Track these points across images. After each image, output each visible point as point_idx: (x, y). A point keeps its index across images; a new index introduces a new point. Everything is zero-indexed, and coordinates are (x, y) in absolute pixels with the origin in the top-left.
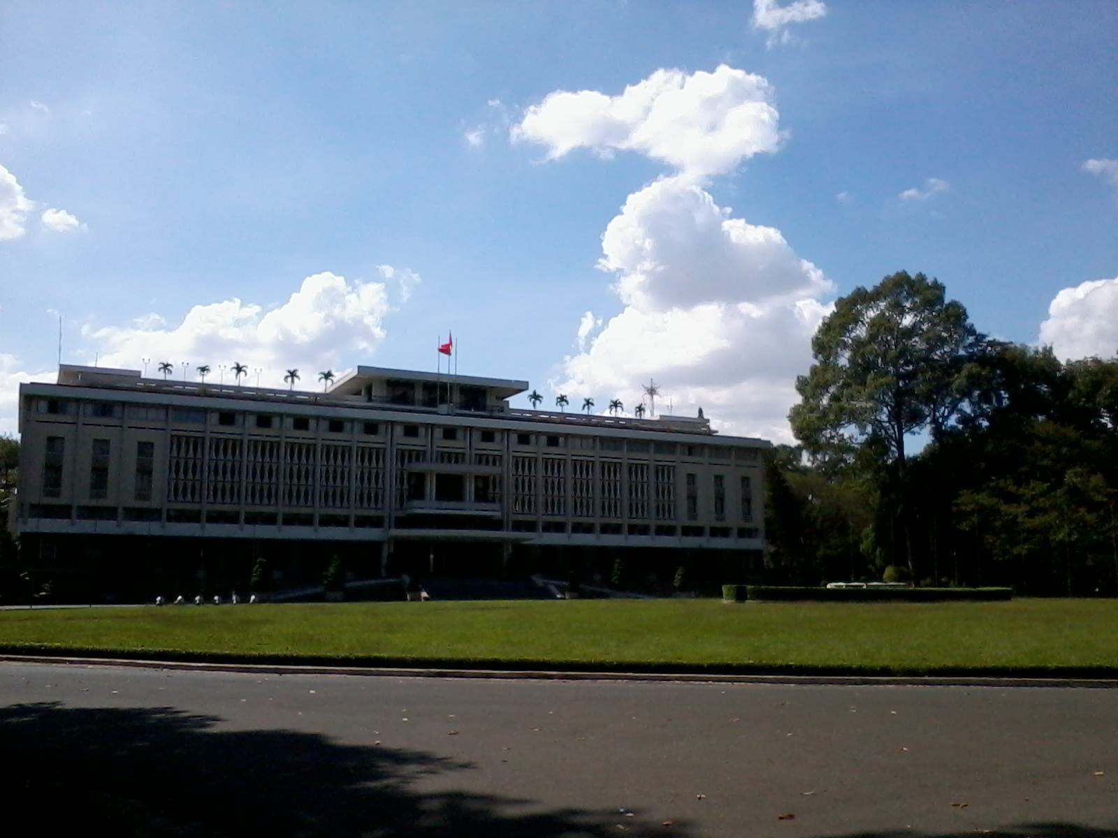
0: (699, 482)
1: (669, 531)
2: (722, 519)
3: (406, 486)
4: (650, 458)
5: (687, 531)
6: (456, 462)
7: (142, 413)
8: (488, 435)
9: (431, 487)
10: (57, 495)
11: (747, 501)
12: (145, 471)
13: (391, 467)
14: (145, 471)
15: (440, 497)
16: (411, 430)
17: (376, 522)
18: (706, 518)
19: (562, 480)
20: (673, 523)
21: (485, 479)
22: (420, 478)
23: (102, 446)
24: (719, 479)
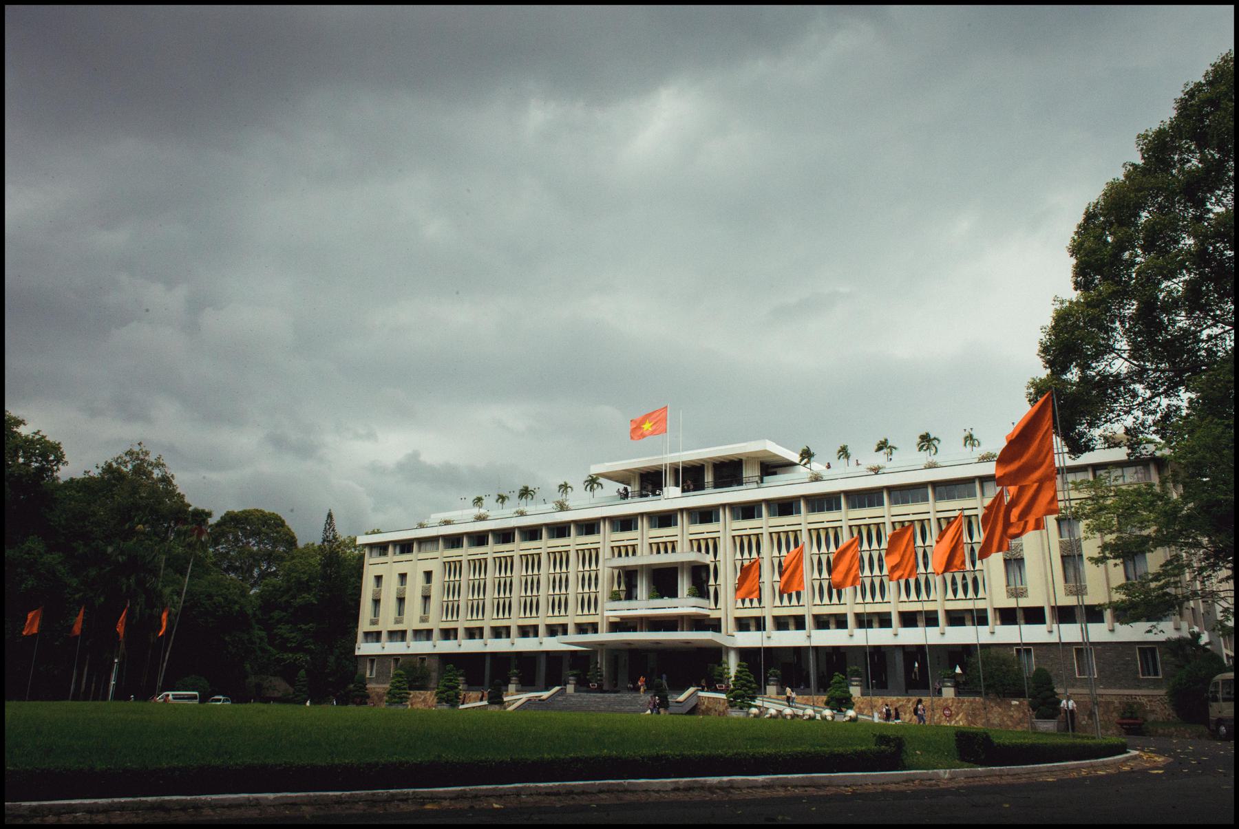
1: (980, 618)
2: (1080, 591)
3: (623, 587)
12: (426, 598)
13: (607, 567)
14: (426, 598)
15: (652, 596)
16: (626, 523)
20: (980, 605)
21: (707, 566)
23: (403, 576)
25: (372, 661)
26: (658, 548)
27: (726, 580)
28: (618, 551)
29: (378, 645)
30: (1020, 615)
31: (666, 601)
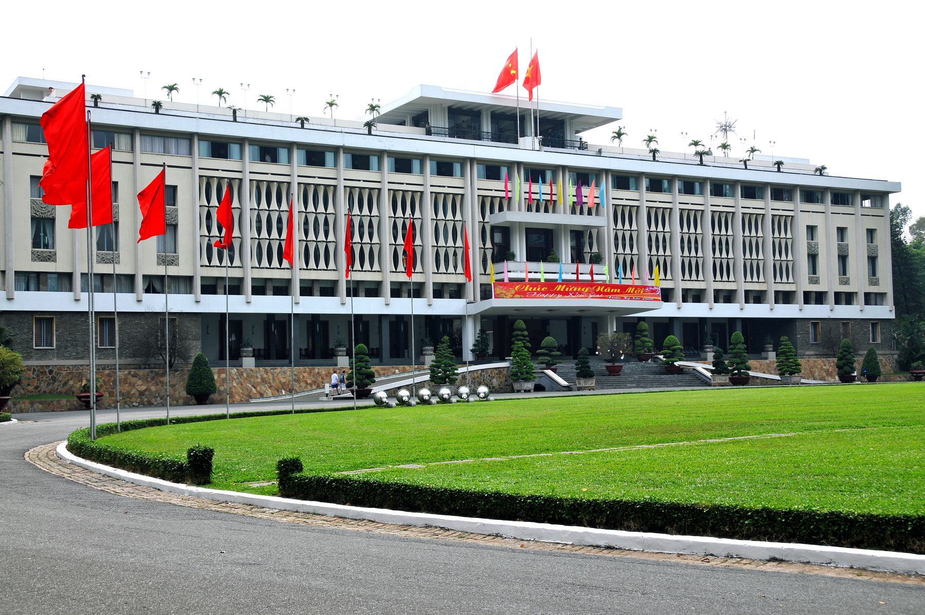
0: (820, 234)
2: (846, 282)
3: (489, 245)
4: (767, 206)
5: (808, 298)
6: (546, 211)
7: (158, 143)
8: (583, 177)
9: (519, 247)
10: (51, 258)
11: (872, 260)
13: (471, 217)
15: (530, 258)
16: (492, 170)
17: (457, 292)
18: (829, 282)
19: (667, 236)
22: (505, 231)
24: (841, 231)
25: (39, 321)
26: (533, 205)
27: (609, 251)
28: (487, 204)
29: (189, 298)
30: (813, 296)
31: (542, 266)
